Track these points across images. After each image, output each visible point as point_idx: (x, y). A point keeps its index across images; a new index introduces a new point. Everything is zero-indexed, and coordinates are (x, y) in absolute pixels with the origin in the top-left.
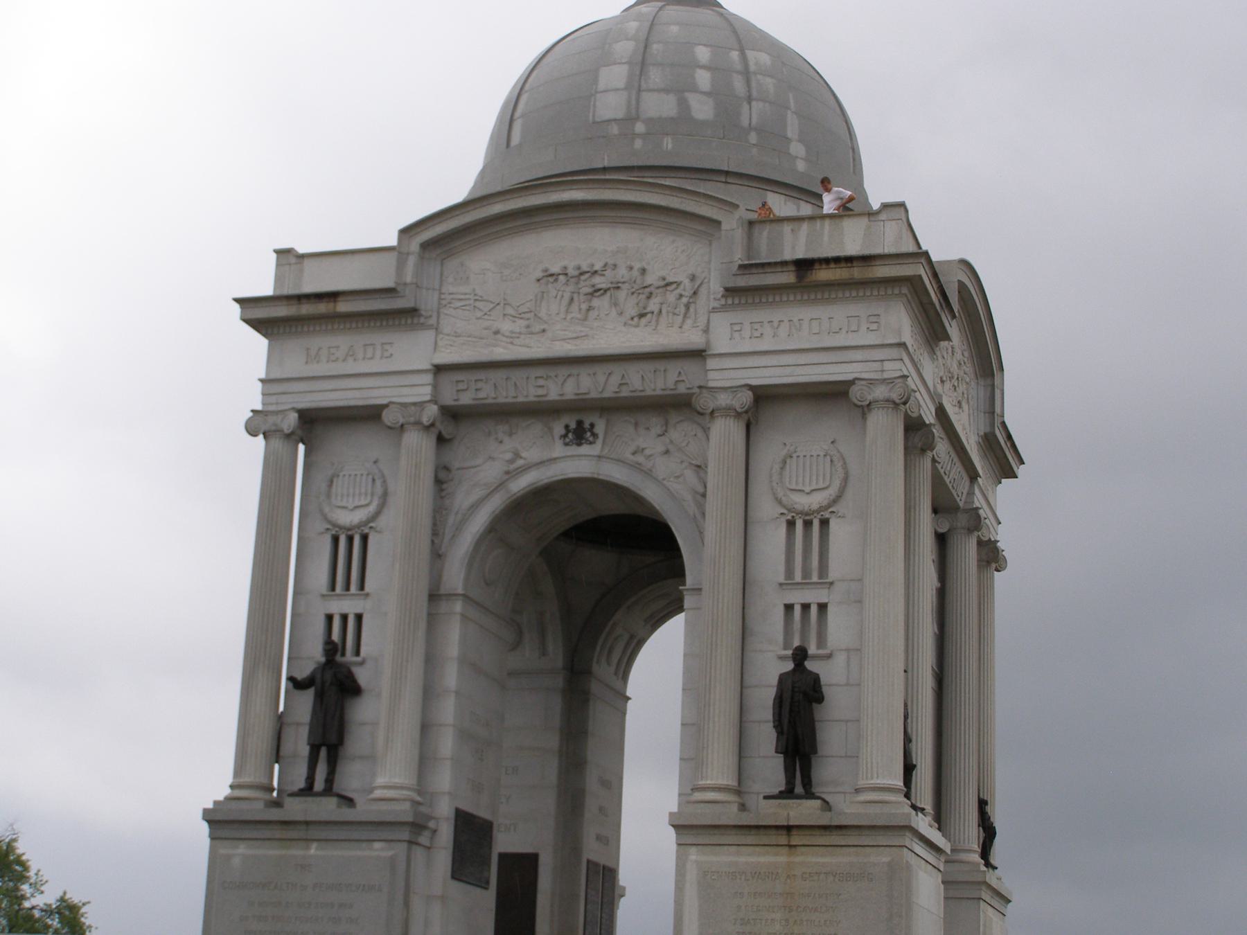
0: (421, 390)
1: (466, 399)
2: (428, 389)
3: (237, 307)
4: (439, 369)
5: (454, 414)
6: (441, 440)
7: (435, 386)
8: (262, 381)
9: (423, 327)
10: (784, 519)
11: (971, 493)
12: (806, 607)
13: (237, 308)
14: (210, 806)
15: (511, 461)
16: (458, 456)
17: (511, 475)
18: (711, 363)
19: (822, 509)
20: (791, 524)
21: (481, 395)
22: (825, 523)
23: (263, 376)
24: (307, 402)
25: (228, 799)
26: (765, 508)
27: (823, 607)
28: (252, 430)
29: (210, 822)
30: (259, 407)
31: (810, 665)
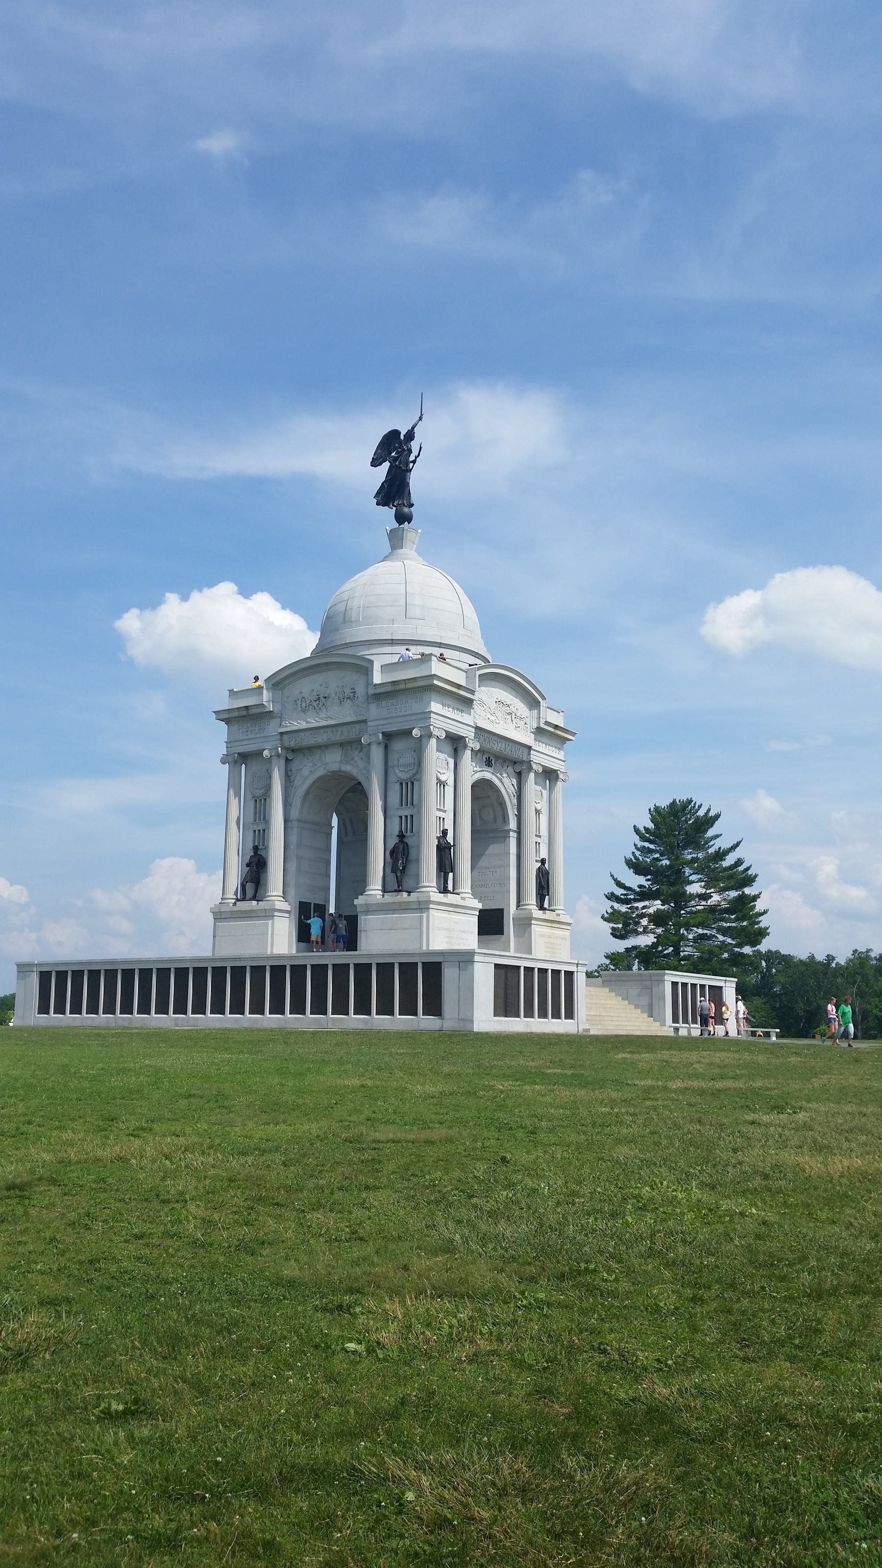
1: (292, 744)
6: (287, 760)
7: (281, 740)
9: (273, 718)
11: (529, 754)
16: (294, 766)
18: (369, 724)
19: (411, 778)
20: (401, 784)
21: (297, 742)
22: (412, 783)
24: (241, 750)
26: (392, 778)
27: (412, 816)
28: (223, 762)
31: (405, 840)
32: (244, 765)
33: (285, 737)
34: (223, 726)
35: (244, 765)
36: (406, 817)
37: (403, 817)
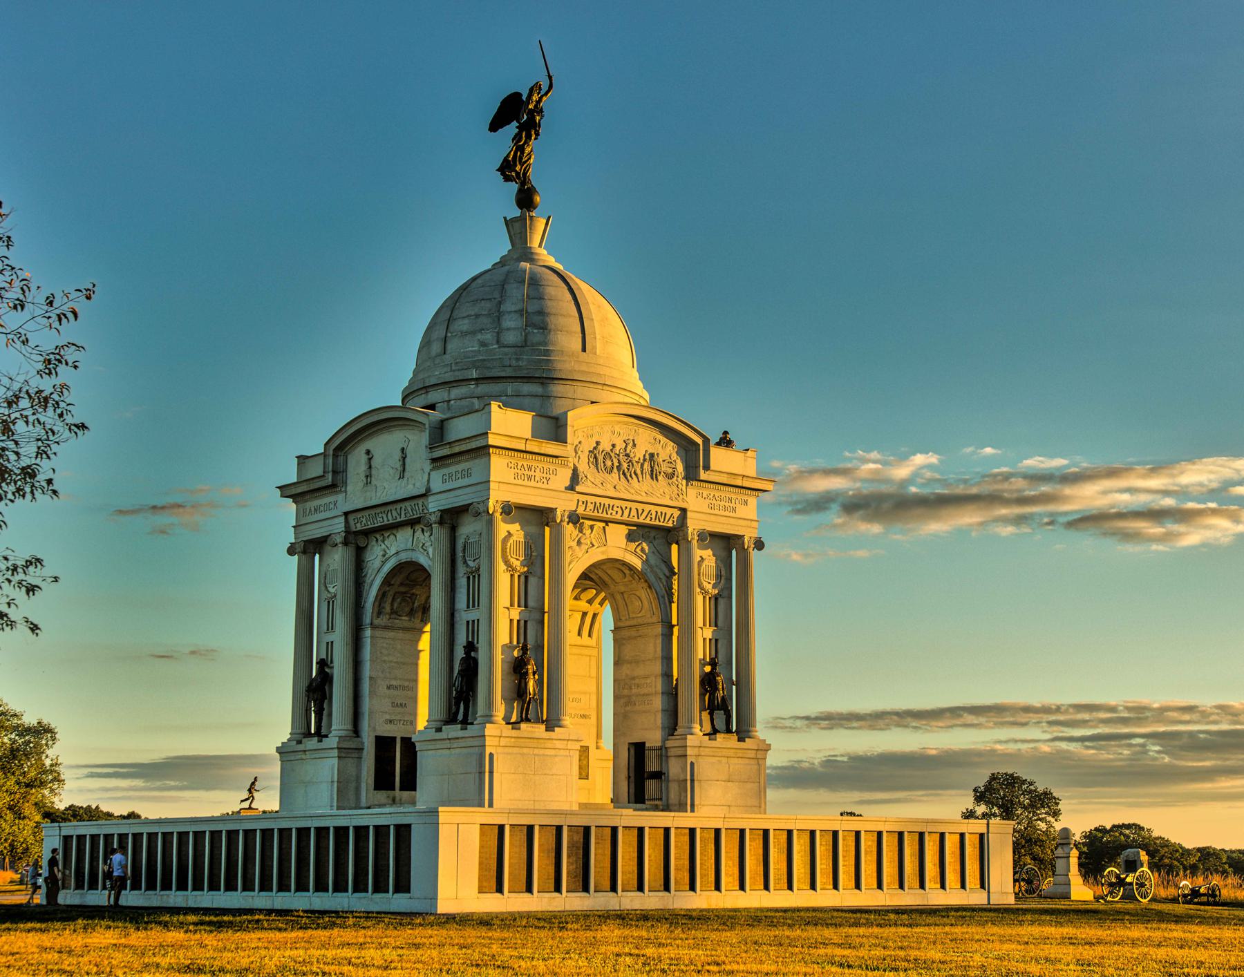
0: (339, 526)
2: (343, 525)
3: (278, 490)
4: (346, 514)
5: (367, 533)
7: (347, 521)
8: (294, 527)
10: (466, 576)
12: (473, 621)
13: (278, 492)
14: (280, 745)
15: (384, 556)
17: (384, 563)
18: (431, 499)
23: (294, 524)
25: (289, 740)
28: (291, 551)
29: (279, 753)
30: (293, 541)
32: (317, 556)
33: (351, 517)
34: (290, 507)
35: (317, 556)
36: (473, 621)
37: (476, 622)
